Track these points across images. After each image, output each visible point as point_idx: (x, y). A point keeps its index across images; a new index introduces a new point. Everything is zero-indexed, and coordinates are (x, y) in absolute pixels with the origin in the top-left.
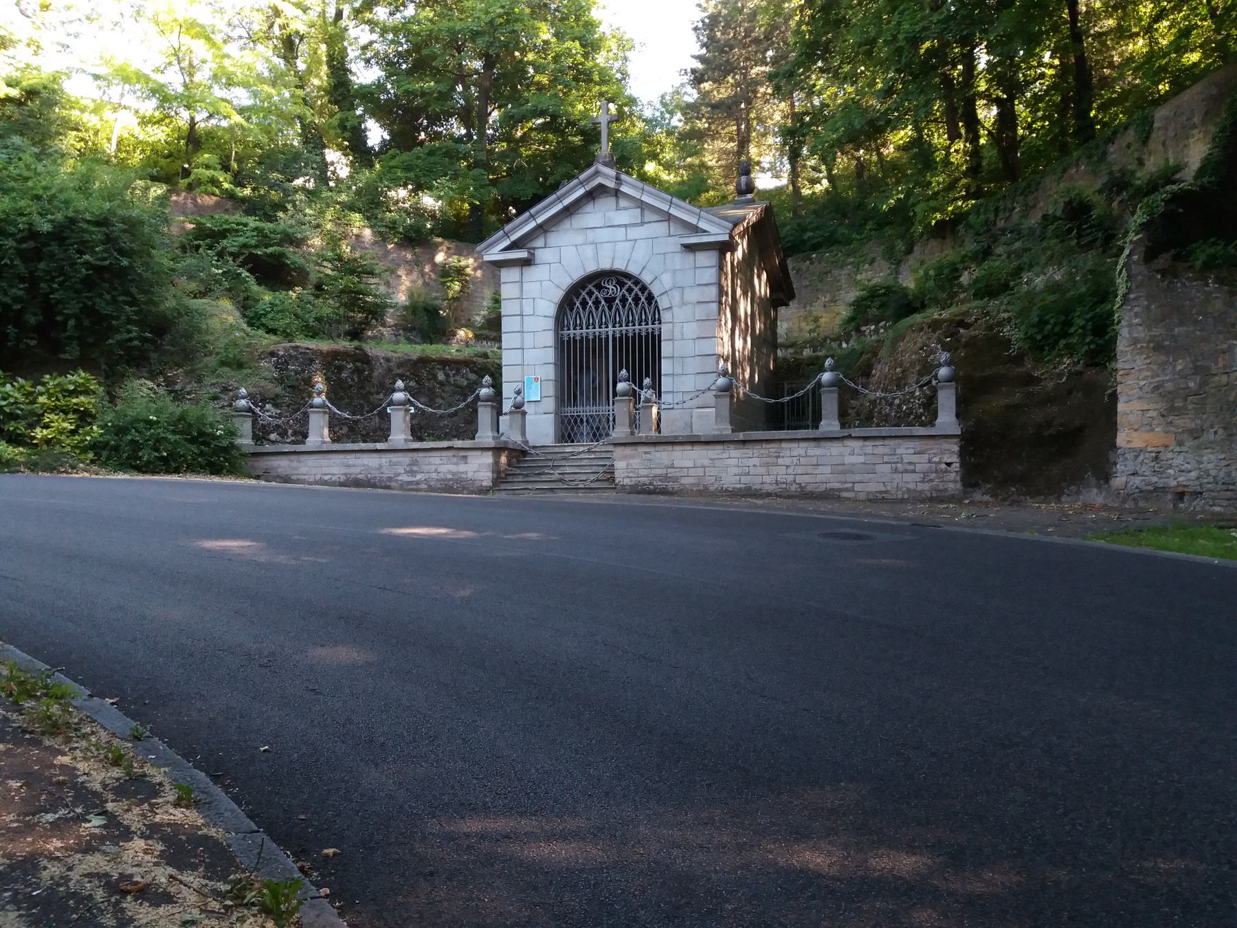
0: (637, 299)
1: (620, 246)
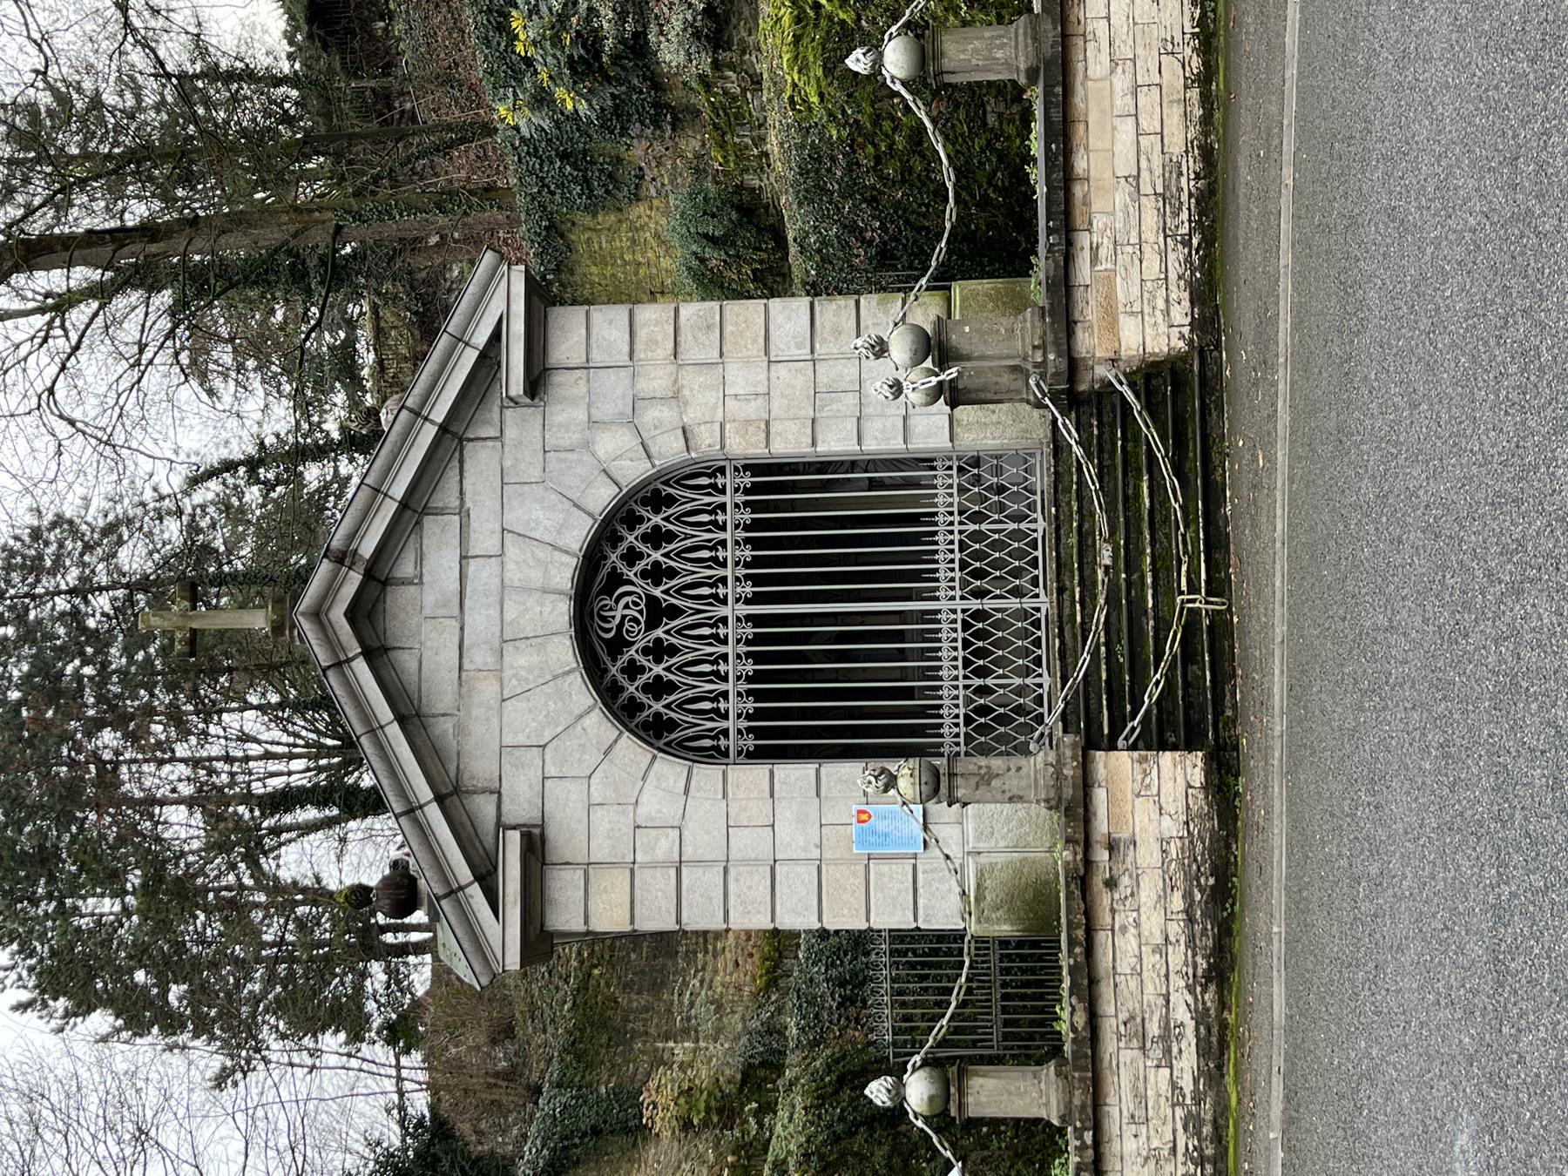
0: (657, 538)
1: (514, 575)
